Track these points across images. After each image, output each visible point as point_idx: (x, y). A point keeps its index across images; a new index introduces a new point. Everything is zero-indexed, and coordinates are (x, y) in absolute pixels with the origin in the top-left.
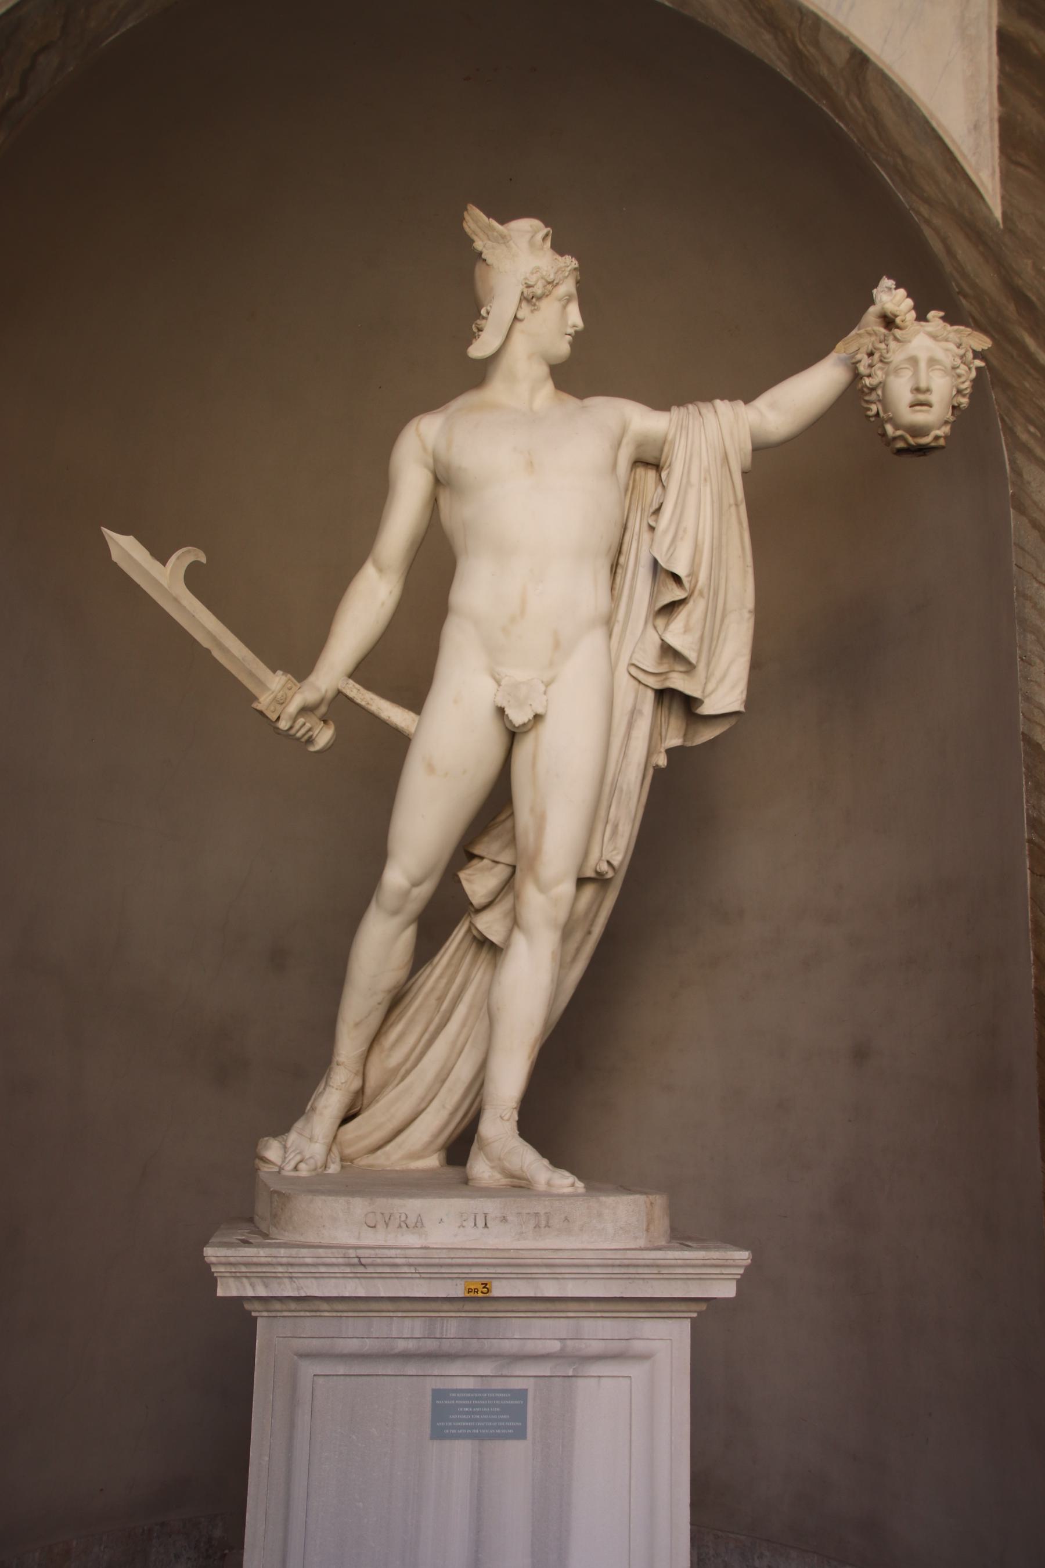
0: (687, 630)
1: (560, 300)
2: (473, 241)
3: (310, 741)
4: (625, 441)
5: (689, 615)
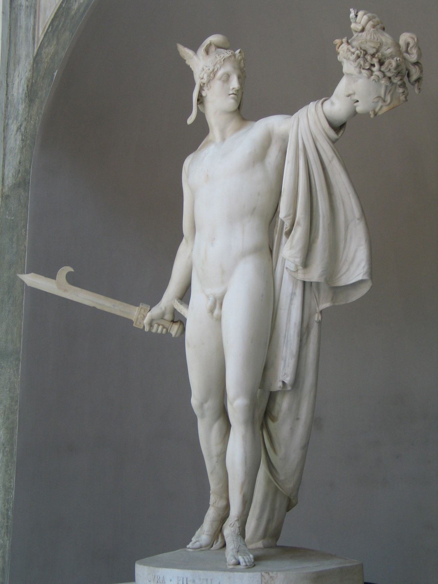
0: (291, 248)
1: (220, 79)
2: (185, 61)
3: (168, 334)
4: (274, 141)
5: (293, 237)
